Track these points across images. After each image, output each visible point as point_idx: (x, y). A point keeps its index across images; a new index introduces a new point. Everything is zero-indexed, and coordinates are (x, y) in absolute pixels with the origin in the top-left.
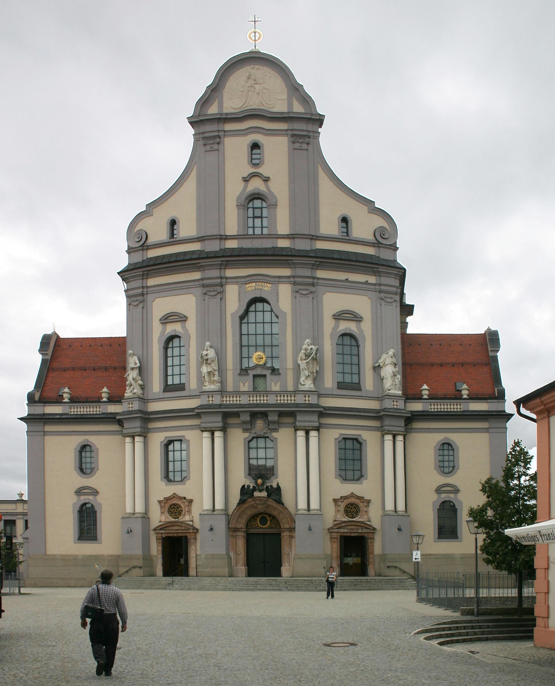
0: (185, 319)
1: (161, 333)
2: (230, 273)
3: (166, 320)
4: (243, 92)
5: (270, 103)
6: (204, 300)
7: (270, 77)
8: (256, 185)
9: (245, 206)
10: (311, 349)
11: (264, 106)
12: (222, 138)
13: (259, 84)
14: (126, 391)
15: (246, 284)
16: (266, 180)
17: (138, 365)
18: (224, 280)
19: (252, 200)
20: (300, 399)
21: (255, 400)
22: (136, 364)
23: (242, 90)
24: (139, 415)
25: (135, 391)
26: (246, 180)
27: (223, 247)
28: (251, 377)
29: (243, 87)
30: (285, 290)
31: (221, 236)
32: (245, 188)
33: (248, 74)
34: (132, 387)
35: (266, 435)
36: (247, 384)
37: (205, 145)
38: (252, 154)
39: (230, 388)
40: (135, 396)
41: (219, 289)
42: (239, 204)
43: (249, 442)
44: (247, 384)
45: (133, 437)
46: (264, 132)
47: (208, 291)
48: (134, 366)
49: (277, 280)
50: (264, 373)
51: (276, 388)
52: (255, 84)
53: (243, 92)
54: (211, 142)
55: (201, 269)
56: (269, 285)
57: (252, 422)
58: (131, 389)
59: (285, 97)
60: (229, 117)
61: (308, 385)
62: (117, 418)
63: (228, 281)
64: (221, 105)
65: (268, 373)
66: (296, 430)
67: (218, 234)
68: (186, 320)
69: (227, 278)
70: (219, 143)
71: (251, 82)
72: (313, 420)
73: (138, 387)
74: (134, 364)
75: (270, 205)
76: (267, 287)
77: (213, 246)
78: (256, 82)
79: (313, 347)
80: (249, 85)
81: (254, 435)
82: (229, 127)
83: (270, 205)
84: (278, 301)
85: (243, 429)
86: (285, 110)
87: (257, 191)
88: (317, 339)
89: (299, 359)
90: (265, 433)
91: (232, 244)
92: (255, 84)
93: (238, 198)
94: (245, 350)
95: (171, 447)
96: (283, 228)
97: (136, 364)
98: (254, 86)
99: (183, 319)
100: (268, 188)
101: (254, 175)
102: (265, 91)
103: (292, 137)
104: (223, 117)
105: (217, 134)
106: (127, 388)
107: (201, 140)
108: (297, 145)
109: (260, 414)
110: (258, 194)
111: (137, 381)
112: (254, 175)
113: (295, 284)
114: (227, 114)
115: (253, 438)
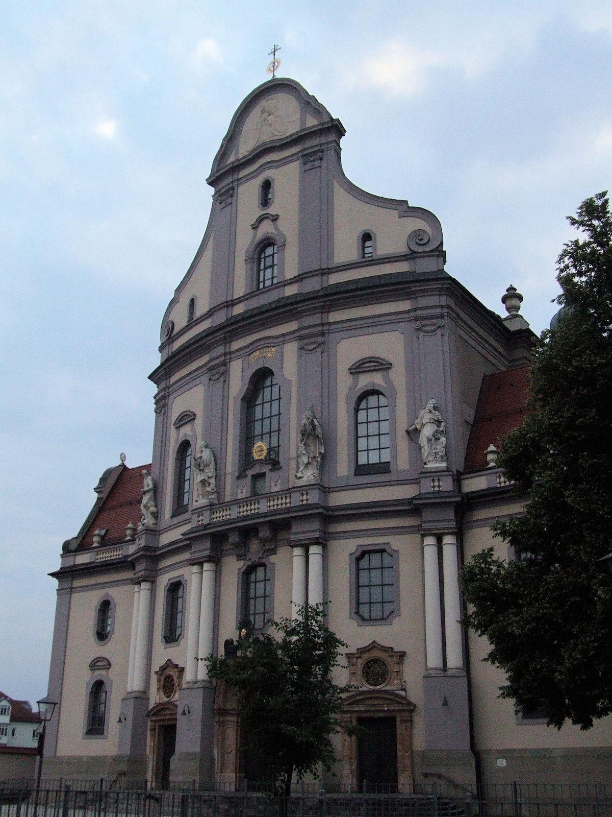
8: (267, 228)
18: (228, 357)
19: (263, 250)
20: (296, 500)
21: (263, 507)
26: (255, 227)
28: (249, 479)
30: (291, 349)
32: (255, 236)
56: (273, 349)
63: (233, 356)
72: (313, 528)
73: (150, 515)
76: (272, 352)
87: (265, 236)
91: (239, 309)
93: (247, 251)
96: (291, 272)
100: (276, 228)
101: (261, 219)
108: (308, 166)
113: (301, 338)
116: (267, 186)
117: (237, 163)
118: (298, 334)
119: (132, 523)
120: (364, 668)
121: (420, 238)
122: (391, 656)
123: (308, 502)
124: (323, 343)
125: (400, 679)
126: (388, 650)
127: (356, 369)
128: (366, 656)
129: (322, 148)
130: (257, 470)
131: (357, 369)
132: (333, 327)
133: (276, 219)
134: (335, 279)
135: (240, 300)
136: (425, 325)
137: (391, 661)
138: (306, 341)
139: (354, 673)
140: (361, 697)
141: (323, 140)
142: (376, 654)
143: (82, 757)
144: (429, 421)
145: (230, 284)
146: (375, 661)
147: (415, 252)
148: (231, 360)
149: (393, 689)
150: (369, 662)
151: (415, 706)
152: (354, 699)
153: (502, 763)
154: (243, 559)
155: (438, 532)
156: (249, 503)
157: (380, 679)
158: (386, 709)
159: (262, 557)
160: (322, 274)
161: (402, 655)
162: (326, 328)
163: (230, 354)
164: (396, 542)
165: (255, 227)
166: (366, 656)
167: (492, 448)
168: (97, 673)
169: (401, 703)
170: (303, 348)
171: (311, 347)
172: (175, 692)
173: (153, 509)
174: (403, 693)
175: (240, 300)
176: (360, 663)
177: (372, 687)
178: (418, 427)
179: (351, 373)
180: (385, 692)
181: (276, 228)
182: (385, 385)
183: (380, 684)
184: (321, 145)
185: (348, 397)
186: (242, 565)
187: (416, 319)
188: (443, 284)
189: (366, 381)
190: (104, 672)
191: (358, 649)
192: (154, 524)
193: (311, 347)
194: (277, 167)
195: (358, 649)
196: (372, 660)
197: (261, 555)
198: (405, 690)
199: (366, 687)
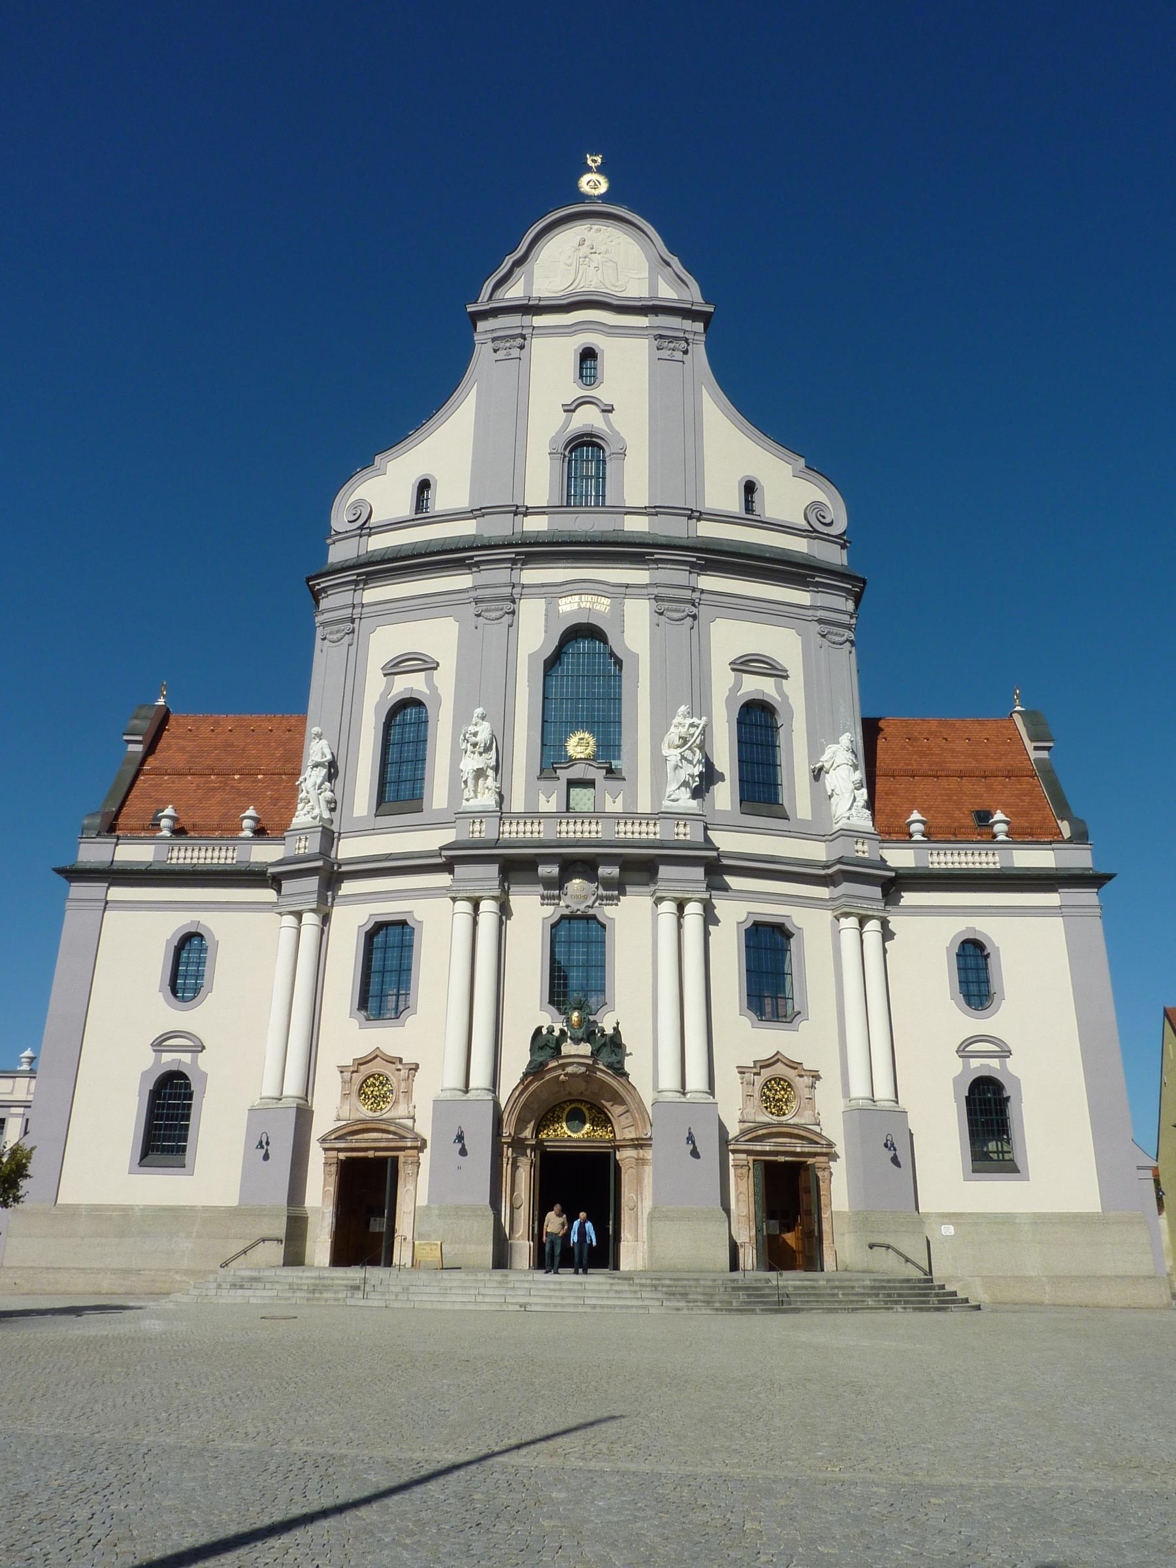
0: (435, 665)
1: (381, 696)
2: (532, 575)
3: (395, 667)
4: (570, 266)
5: (617, 284)
6: (476, 628)
7: (619, 244)
8: (587, 419)
9: (565, 456)
10: (692, 725)
11: (607, 288)
12: (529, 339)
13: (599, 254)
14: (297, 813)
15: (560, 598)
16: (608, 410)
17: (329, 757)
18: (517, 590)
21: (571, 830)
22: (323, 755)
23: (569, 262)
24: (320, 863)
25: (316, 812)
26: (570, 410)
27: (517, 529)
28: (563, 784)
29: (570, 257)
31: (517, 507)
32: (567, 423)
33: (579, 238)
34: (309, 804)
35: (591, 912)
36: (554, 798)
37: (495, 351)
38: (581, 368)
39: (517, 804)
40: (316, 822)
41: (508, 606)
42: (555, 451)
43: (553, 926)
44: (554, 798)
45: (299, 915)
46: (606, 330)
47: (487, 611)
48: (319, 760)
49: (623, 590)
50: (589, 776)
51: (614, 805)
52: (591, 253)
53: (570, 266)
54: (508, 345)
55: (474, 569)
56: (607, 601)
57: (559, 884)
58: (307, 808)
59: (646, 274)
60: (542, 303)
61: (686, 802)
62: (271, 870)
63: (525, 591)
64: (529, 284)
65: (598, 775)
66: (658, 901)
67: (512, 504)
68: (435, 669)
69: (523, 586)
70: (522, 347)
71: (584, 250)
73: (323, 804)
74: (320, 755)
75: (613, 454)
77: (499, 527)
78: (593, 251)
79: (695, 720)
80: (581, 255)
81: (567, 912)
82: (539, 320)
83: (613, 454)
84: (623, 632)
85: (543, 897)
86: (644, 292)
87: (588, 430)
88: (700, 705)
89: (664, 747)
90: (588, 906)
91: (536, 525)
92: (591, 253)
93: (553, 441)
94: (552, 728)
95: (378, 940)
97: (323, 755)
98: (590, 256)
99: (429, 666)
100: (608, 423)
101: (582, 402)
102: (609, 264)
103: (656, 340)
104: (531, 303)
105: (518, 331)
106: (300, 806)
107: (490, 345)
108: (665, 354)
109: (579, 863)
110: (592, 435)
111: (321, 792)
112: (582, 402)
113: (657, 598)
114: (540, 299)
115: (563, 917)
116: (588, 355)
117: (537, 302)
118: (656, 591)
119: (254, 809)
120: (763, 1088)
121: (823, 514)
122: (801, 1076)
123: (688, 838)
124: (694, 617)
125: (813, 1109)
126: (793, 1065)
127: (741, 663)
128: (767, 1073)
129: (686, 336)
130: (577, 772)
131: (744, 665)
132: (704, 596)
133: (610, 411)
134: (707, 530)
135: (539, 511)
136: (832, 633)
137: (801, 1083)
138: (666, 605)
139: (751, 1096)
140: (764, 1131)
141: (688, 324)
142: (780, 1070)
143: (131, 1207)
144: (846, 762)
145: (517, 477)
146: (778, 1080)
147: (816, 531)
148: (523, 597)
149: (803, 1122)
150: (770, 1081)
151: (830, 1145)
152: (754, 1134)
153: (948, 1230)
154: (554, 904)
155: (861, 912)
156: (595, 821)
157: (784, 1107)
158: (798, 1150)
159: (592, 907)
160: (690, 517)
161: (817, 1077)
162: (696, 595)
163: (523, 588)
164: (799, 918)
165: (570, 410)
166: (767, 1073)
167: (916, 815)
168: (167, 1057)
169: (818, 1143)
170: (661, 614)
171: (676, 615)
172: (396, 1102)
173: (328, 794)
174: (817, 1129)
175: (539, 511)
176: (759, 1081)
177: (775, 1117)
178: (827, 766)
179: (733, 670)
180: (795, 1126)
181: (608, 423)
182: (779, 699)
183: (784, 1114)
184: (685, 331)
185: (728, 701)
186: (552, 911)
187: (821, 621)
188: (854, 586)
189: (756, 686)
190: (186, 1058)
191: (755, 1062)
192: (328, 819)
193: (676, 615)
194: (608, 334)
195: (755, 1062)
196: (774, 1079)
197: (590, 903)
198: (819, 1125)
199: (766, 1118)
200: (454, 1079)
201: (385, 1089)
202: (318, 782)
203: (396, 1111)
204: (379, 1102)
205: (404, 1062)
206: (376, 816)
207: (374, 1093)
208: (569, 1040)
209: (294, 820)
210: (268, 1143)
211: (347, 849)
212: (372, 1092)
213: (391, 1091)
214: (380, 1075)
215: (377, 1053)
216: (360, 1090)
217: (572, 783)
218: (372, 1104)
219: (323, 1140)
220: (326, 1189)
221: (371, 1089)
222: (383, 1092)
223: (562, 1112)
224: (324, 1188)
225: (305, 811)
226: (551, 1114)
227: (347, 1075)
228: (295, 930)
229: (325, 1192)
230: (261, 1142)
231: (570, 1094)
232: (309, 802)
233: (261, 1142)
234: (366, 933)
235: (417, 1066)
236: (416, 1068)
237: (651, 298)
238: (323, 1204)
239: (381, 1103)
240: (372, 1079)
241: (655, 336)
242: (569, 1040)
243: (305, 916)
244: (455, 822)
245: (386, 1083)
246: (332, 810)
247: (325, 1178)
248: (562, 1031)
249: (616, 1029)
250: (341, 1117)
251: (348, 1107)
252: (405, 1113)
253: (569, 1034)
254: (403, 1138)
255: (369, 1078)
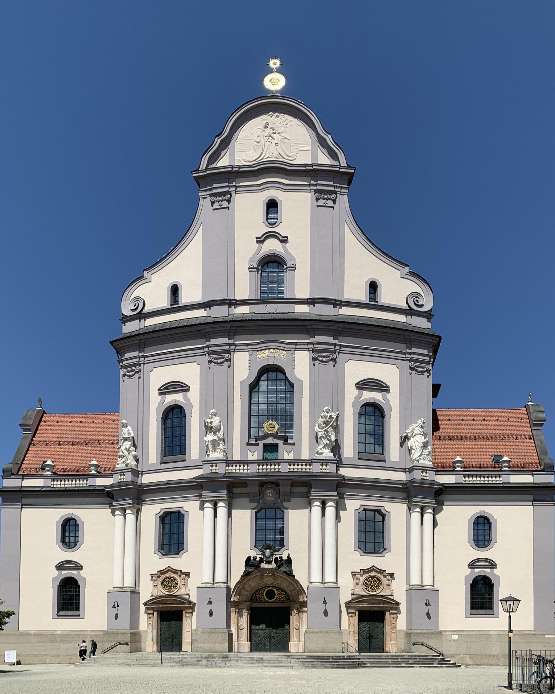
130: (270, 440)
200: (208, 578)
201: (174, 583)
202: (127, 448)
203: (181, 591)
204: (172, 588)
205: (182, 572)
206: (161, 463)
207: (169, 585)
208: (265, 562)
209: (117, 466)
210: (118, 606)
211: (146, 479)
212: (168, 584)
213: (177, 584)
214: (171, 577)
215: (169, 568)
216: (162, 583)
217: (265, 446)
218: (168, 589)
219: (145, 604)
220: (149, 623)
221: (168, 583)
222: (173, 584)
223: (264, 591)
224: (148, 623)
225: (122, 461)
226: (258, 592)
227: (155, 578)
228: (123, 517)
229: (148, 624)
230: (114, 605)
231: (266, 584)
232: (124, 457)
233: (114, 605)
234: (160, 517)
235: (189, 573)
236: (188, 575)
237: (312, 165)
238: (148, 629)
239: (173, 589)
240: (167, 579)
241: (315, 190)
242: (265, 562)
243: (128, 511)
244: (202, 465)
245: (175, 580)
246: (137, 461)
247: (148, 619)
248: (260, 558)
249: (289, 557)
250: (153, 595)
251: (157, 591)
252: (185, 593)
253: (264, 559)
254: (184, 603)
255: (166, 578)
